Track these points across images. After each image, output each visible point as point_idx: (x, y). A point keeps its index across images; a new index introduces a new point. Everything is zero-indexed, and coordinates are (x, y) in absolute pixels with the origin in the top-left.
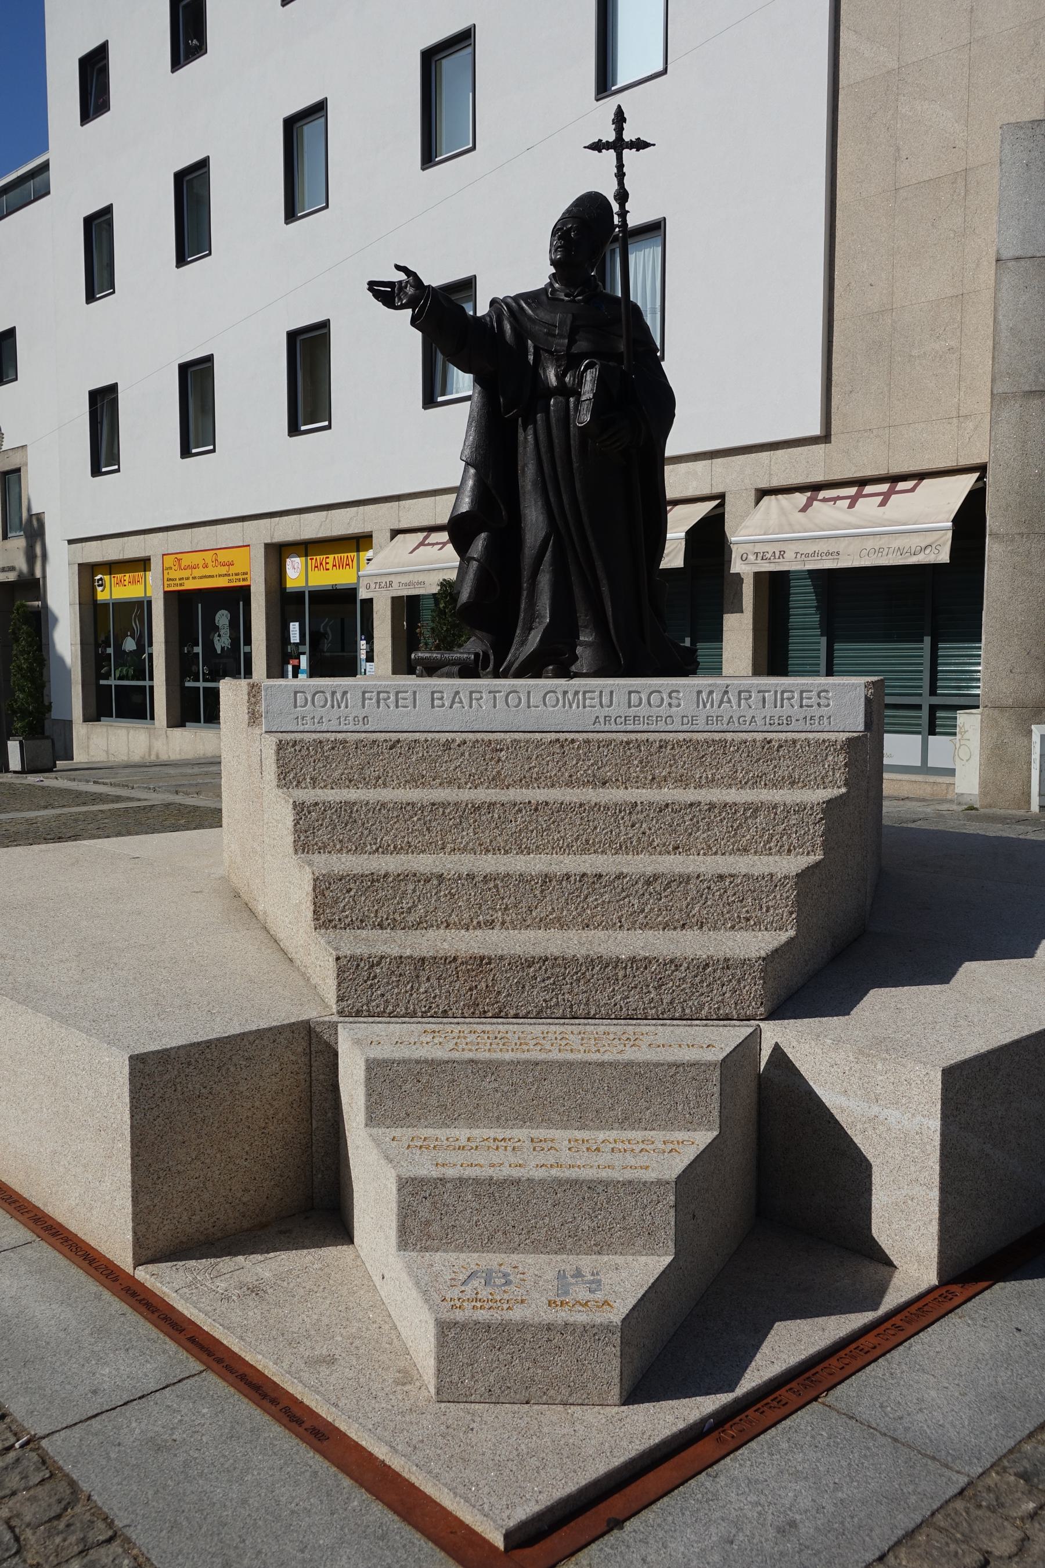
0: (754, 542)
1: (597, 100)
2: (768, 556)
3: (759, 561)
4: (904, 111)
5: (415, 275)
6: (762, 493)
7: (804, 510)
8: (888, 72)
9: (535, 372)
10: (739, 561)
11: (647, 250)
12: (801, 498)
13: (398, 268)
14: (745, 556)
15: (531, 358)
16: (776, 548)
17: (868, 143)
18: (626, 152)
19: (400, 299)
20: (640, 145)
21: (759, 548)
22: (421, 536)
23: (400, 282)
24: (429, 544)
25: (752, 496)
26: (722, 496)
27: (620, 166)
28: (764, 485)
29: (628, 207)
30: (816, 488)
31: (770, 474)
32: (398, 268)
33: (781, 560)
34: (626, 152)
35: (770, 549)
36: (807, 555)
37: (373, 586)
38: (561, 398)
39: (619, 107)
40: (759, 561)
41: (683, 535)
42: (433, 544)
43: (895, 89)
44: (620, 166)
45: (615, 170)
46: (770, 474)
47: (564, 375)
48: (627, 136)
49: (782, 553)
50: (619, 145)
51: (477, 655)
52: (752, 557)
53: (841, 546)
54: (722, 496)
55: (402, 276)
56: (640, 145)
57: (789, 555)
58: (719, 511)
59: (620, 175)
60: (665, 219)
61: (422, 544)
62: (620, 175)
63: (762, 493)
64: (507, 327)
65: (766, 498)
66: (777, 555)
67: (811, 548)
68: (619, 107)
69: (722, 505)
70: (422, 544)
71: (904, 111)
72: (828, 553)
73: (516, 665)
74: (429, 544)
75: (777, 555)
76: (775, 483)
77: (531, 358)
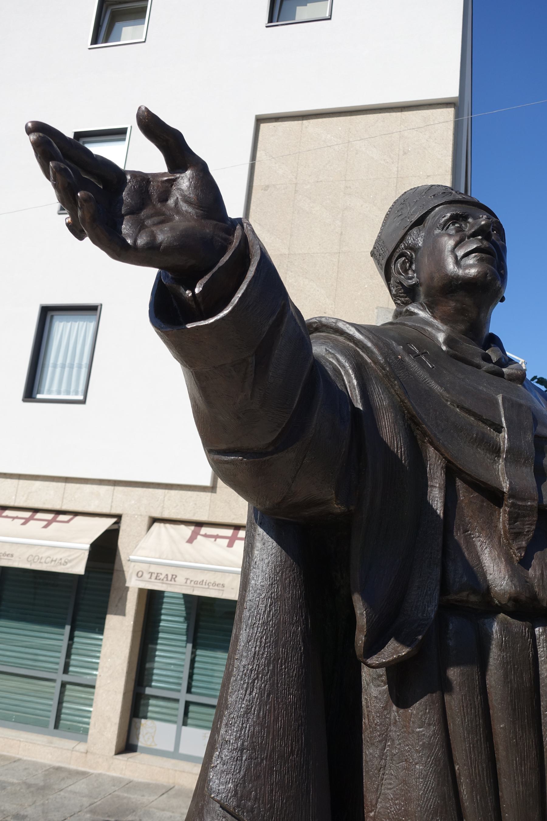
0: (150, 563)
1: (59, 214)
2: (162, 577)
3: (153, 579)
4: (290, 281)
5: (201, 168)
6: (154, 520)
7: (191, 540)
8: (281, 255)
9: (444, 542)
10: (134, 577)
11: (81, 323)
12: (188, 531)
13: (152, 126)
14: (140, 574)
15: (436, 499)
16: (170, 572)
19: (140, 227)
21: (153, 569)
23: (143, 180)
26: (119, 517)
28: (157, 515)
30: (199, 524)
31: (163, 507)
33: (173, 582)
35: (164, 571)
36: (196, 582)
38: (516, 625)
40: (153, 579)
41: (88, 546)
43: (285, 266)
46: (163, 507)
47: (525, 563)
49: (174, 577)
52: (146, 576)
54: (119, 517)
57: (180, 579)
58: (116, 527)
60: (101, 305)
63: (154, 520)
64: (381, 399)
65: (156, 525)
66: (169, 578)
67: (200, 577)
69: (118, 523)
71: (290, 281)
72: (214, 584)
75: (169, 578)
76: (166, 515)
77: (436, 499)
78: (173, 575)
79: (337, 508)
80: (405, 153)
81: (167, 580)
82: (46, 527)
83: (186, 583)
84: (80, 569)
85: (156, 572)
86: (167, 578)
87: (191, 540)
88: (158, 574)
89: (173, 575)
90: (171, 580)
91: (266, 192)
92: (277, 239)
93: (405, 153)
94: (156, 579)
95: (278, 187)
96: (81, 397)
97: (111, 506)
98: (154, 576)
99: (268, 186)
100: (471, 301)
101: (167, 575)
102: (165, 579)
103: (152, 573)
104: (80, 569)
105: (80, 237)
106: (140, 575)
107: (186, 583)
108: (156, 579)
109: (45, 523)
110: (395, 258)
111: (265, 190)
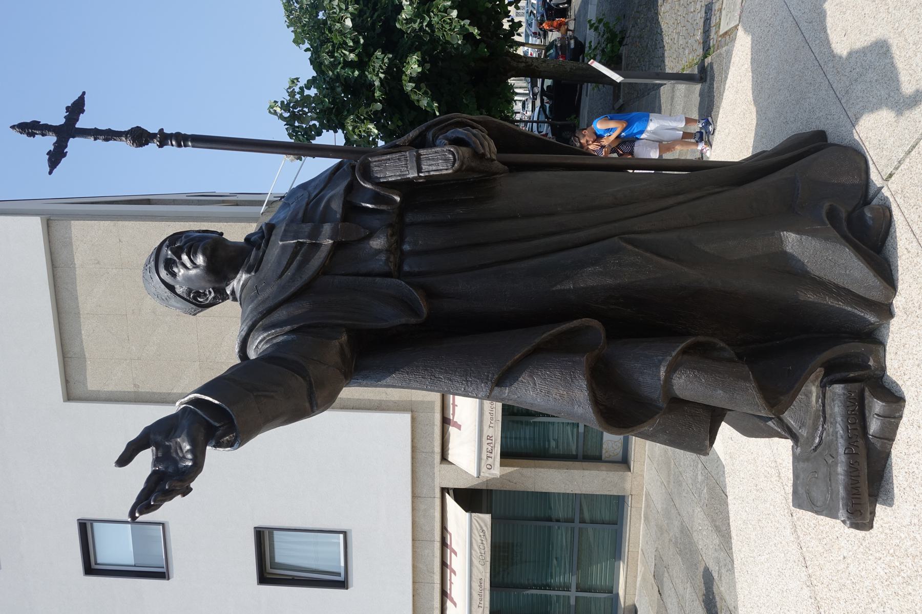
3: (492, 455)
7: (459, 427)
10: (492, 471)
13: (124, 460)
25: (445, 466)
26: (444, 490)
27: (95, 133)
29: (153, 129)
32: (124, 460)
36: (492, 419)
39: (13, 127)
40: (492, 455)
44: (95, 133)
49: (489, 438)
50: (67, 131)
52: (490, 461)
55: (145, 460)
58: (451, 492)
59: (109, 135)
62: (109, 135)
68: (13, 127)
79: (344, 338)
80: (98, 263)
82: (456, 554)
84: (487, 517)
87: (459, 427)
93: (98, 263)
96: (341, 536)
100: (223, 260)
104: (487, 517)
105: (190, 490)
109: (453, 555)
110: (197, 301)
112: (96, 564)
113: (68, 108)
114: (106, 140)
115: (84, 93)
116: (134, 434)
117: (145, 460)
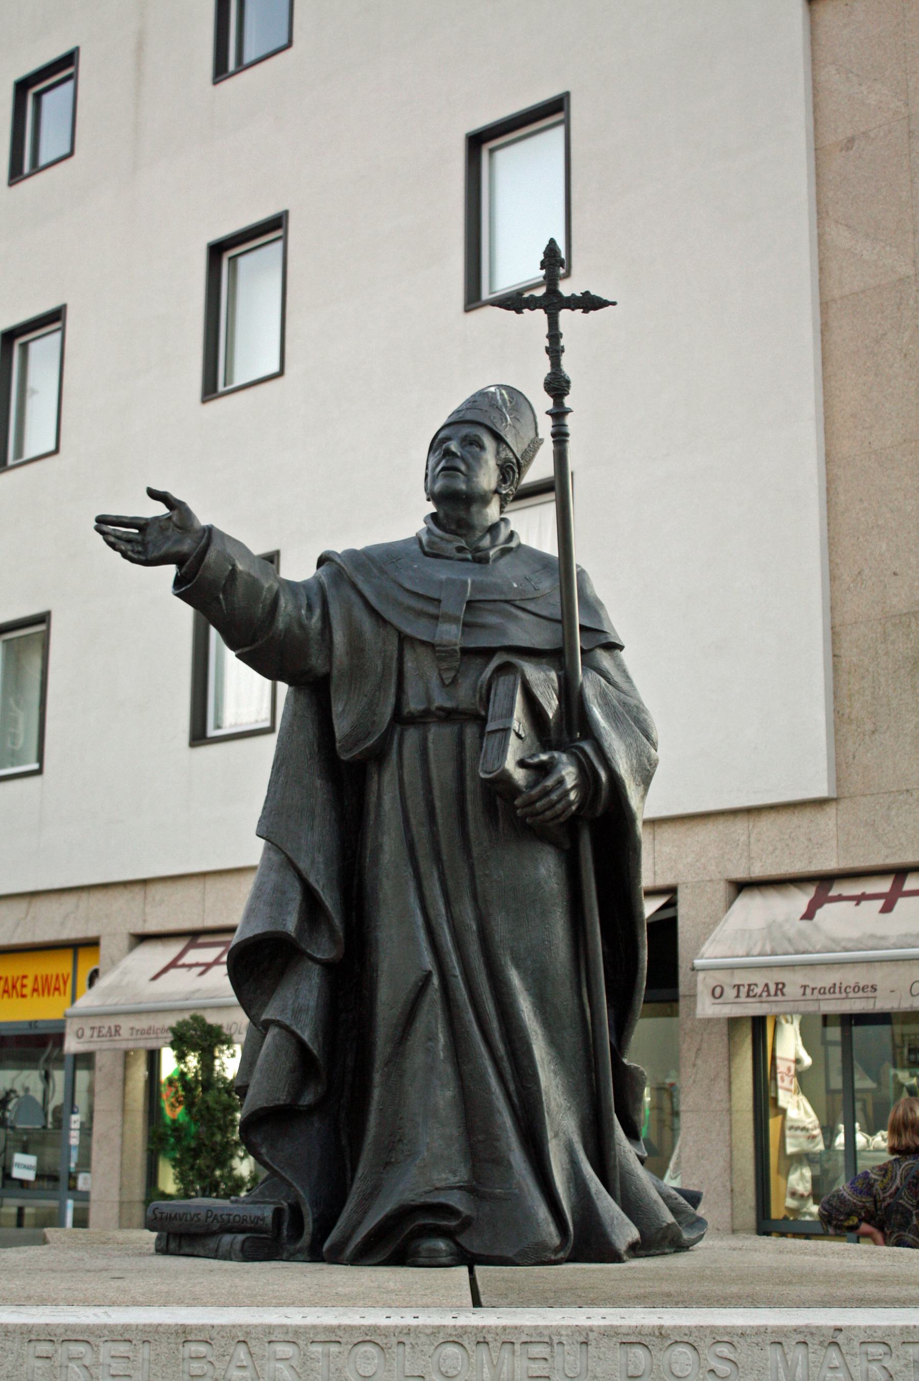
0: (732, 968)
2: (758, 990)
3: (743, 998)
6: (741, 887)
7: (809, 915)
8: (901, 280)
13: (154, 494)
17: (876, 375)
18: (565, 315)
20: (589, 303)
21: (743, 978)
22: (172, 950)
24: (184, 966)
25: (721, 891)
27: (554, 335)
29: (568, 402)
32: (154, 494)
33: (780, 998)
34: (565, 315)
35: (760, 979)
36: (822, 991)
37: (88, 1033)
40: (743, 998)
42: (190, 966)
43: (911, 302)
44: (554, 335)
45: (546, 343)
46: (750, 858)
48: (566, 288)
49: (780, 988)
50: (553, 303)
51: (278, 1213)
52: (730, 993)
53: (877, 976)
55: (159, 509)
56: (589, 303)
59: (555, 351)
61: (173, 965)
62: (555, 351)
63: (741, 887)
66: (772, 991)
67: (827, 979)
69: (672, 904)
70: (173, 965)
72: (857, 988)
73: (358, 1238)
74: (184, 966)
75: (772, 991)
76: (758, 871)
78: (777, 984)
81: (769, 995)
83: (804, 994)
85: (746, 983)
86: (768, 991)
87: (809, 915)
88: (749, 985)
89: (777, 984)
90: (776, 995)
91: (851, 153)
92: (888, 249)
94: (748, 996)
95: (872, 135)
97: (655, 873)
98: (744, 990)
99: (851, 140)
101: (767, 985)
102: (765, 994)
103: (739, 986)
106: (717, 993)
107: (804, 994)
108: (748, 996)
111: (848, 149)
112: (492, 151)
113: (587, 293)
114: (548, 350)
115: (614, 304)
116: (178, 494)
117: (159, 509)
